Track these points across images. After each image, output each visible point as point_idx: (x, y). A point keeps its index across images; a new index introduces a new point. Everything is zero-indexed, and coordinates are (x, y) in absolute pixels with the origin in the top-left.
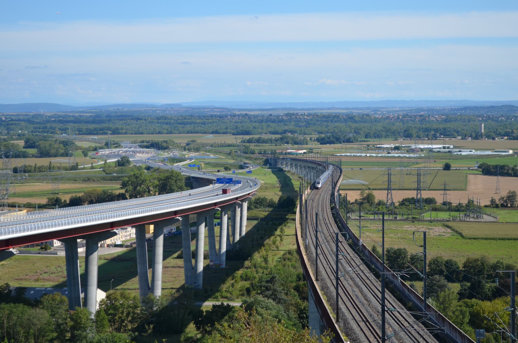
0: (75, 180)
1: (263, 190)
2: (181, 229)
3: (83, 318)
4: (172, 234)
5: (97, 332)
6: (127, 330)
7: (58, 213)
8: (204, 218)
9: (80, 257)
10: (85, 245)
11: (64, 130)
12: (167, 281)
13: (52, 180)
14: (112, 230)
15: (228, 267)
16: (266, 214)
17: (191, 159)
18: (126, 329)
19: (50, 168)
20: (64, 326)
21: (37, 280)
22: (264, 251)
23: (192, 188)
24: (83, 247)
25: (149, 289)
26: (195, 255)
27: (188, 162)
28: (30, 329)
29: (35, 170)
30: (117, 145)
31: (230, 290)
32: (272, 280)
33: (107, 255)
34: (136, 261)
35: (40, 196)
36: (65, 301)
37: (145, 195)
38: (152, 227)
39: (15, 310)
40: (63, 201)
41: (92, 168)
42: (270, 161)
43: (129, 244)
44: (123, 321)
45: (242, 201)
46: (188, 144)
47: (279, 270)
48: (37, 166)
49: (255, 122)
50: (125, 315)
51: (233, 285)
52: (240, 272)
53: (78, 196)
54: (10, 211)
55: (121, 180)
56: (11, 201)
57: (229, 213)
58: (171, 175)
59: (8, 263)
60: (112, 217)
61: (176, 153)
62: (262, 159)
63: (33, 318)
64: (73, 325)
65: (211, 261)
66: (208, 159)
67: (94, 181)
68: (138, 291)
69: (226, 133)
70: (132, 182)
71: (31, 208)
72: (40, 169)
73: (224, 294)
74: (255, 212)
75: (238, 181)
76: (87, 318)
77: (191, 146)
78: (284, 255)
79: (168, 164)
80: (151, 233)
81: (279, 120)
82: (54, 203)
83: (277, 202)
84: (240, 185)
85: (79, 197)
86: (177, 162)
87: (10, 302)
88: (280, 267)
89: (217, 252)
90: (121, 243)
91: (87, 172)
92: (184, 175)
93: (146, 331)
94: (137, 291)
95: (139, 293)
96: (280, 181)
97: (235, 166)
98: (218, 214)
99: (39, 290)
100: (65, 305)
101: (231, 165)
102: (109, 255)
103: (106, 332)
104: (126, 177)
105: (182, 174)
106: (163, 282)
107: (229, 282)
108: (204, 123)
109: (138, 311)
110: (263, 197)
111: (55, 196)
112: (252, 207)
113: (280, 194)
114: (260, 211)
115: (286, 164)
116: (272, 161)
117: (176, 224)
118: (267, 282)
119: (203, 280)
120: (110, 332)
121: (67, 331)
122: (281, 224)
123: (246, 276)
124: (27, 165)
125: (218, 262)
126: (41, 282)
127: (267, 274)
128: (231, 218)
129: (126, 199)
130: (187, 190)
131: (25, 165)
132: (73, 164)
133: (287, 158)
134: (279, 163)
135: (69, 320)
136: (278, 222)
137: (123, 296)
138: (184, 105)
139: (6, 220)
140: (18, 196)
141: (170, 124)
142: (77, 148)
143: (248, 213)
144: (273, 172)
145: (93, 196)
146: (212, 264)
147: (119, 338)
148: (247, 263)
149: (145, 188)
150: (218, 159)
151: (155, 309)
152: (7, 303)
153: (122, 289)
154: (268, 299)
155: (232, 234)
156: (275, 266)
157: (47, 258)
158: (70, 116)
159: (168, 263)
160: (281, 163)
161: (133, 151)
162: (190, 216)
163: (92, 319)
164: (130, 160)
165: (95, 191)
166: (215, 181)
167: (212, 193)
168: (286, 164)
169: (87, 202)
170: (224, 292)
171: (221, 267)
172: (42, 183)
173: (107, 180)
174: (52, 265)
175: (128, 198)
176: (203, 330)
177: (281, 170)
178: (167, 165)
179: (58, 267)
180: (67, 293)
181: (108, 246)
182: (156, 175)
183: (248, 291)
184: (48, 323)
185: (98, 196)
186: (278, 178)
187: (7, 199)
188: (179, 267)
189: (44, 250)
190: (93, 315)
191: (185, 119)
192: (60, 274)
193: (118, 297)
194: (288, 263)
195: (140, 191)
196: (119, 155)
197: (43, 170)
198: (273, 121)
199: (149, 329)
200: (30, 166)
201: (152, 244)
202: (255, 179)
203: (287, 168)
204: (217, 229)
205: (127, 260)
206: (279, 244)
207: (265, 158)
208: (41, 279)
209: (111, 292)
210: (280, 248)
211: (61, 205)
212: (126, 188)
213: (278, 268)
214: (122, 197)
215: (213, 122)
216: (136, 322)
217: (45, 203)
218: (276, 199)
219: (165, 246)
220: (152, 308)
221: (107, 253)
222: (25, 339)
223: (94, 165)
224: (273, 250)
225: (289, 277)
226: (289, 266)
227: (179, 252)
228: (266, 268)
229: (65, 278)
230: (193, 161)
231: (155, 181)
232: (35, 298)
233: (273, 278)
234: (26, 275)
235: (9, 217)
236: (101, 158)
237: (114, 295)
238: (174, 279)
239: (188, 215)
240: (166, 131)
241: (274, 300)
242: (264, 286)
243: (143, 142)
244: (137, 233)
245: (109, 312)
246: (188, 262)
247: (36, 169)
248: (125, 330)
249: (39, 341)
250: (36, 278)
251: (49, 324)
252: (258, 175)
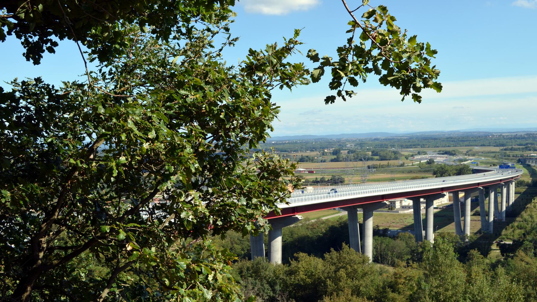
11: (393, 146)
17: (471, 160)
30: (425, 153)
41: (413, 165)
46: (467, 152)
49: (507, 139)
61: (461, 157)
69: (490, 146)
72: (382, 166)
77: (470, 153)
81: (522, 138)
96: (529, 172)
108: (475, 141)
138: (461, 131)
141: (454, 141)
142: (403, 155)
144: (524, 167)
158: (395, 139)
160: (529, 162)
161: (435, 156)
177: (529, 165)
191: (463, 138)
196: (426, 159)
198: (519, 138)
200: (377, 165)
215: (481, 140)
236: (416, 160)
240: (452, 146)
243: (440, 151)
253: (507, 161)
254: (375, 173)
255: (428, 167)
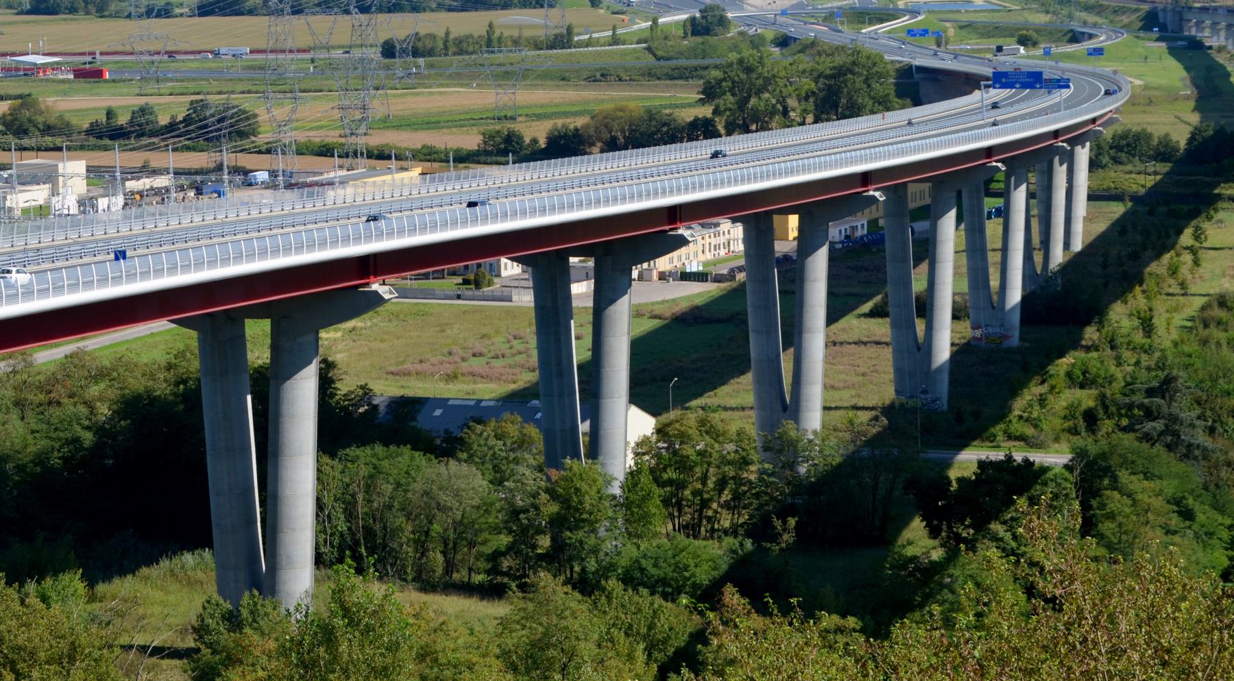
0: (563, 79)
1: (1140, 108)
2: (882, 228)
3: (587, 493)
4: (855, 242)
5: (630, 534)
6: (718, 530)
7: (513, 180)
8: (954, 194)
9: (578, 307)
10: (592, 273)
12: (841, 385)
13: (496, 77)
14: (671, 230)
15: (1027, 344)
16: (1150, 181)
18: (716, 526)
19: (489, 43)
20: (532, 513)
21: (452, 377)
22: (1140, 296)
23: (917, 102)
24: (587, 278)
25: (785, 408)
26: (925, 307)
27: (904, 21)
28: (431, 522)
29: (446, 48)
31: (1035, 415)
32: (1165, 388)
33: (658, 303)
34: (745, 322)
35: (462, 126)
36: (531, 443)
37: (774, 124)
38: (793, 220)
39: (385, 463)
40: (527, 140)
41: (615, 41)
42: (1161, 15)
43: (725, 272)
44: (705, 504)
45: (1074, 142)
47: (1190, 356)
48: (452, 36)
50: (711, 484)
51: (1042, 401)
52: (1065, 362)
53: (572, 127)
54: (373, 172)
55: (701, 77)
56: (376, 140)
57: (1033, 178)
58: (854, 63)
59: (369, 324)
60: (671, 192)
62: (1137, 10)
63: (440, 489)
64: (558, 513)
65: (975, 327)
66: (966, 11)
67: (620, 80)
68: (752, 413)
70: (733, 82)
71: (434, 161)
72: (461, 46)
73: (1018, 427)
74: (1112, 174)
75: (1058, 81)
76: (599, 492)
78: (1203, 309)
79: (845, 28)
80: (791, 238)
82: (502, 146)
83: (1183, 144)
84: (1065, 93)
85: (576, 129)
86: (871, 23)
87: (374, 443)
88: (1192, 347)
89: (995, 298)
90: (701, 268)
91: (599, 54)
92: (892, 62)
93: (775, 538)
94: (747, 412)
95: (753, 420)
97: (1050, 33)
98: (998, 181)
99: (459, 406)
100: (535, 451)
101: (1037, 31)
102: (666, 305)
103: (656, 535)
104: (716, 67)
105: (887, 58)
106: (826, 387)
107: (1035, 390)
109: (751, 474)
110: (1139, 129)
111: (505, 127)
112: (1105, 159)
113: (1195, 118)
114: (1131, 172)
115: (1214, 25)
116: (1169, 16)
117: (867, 211)
118: (1150, 392)
119: (951, 383)
120: (668, 534)
121: (540, 531)
122: (1195, 214)
123: (1084, 374)
124: (422, 32)
125: (998, 330)
126: (464, 382)
127: (1149, 369)
128: (1038, 194)
129: (720, 136)
130: (903, 107)
131: (417, 34)
132: (557, 31)
133: (1216, 9)
134: (1192, 24)
135: (544, 497)
136: (1186, 208)
137: (706, 427)
139: (359, 199)
140: (398, 127)
143: (1090, 178)
144: (1173, 52)
145: (616, 126)
146: (978, 333)
147: (696, 556)
148: (1090, 334)
149: (774, 101)
150: (999, 11)
151: (803, 469)
152: (364, 445)
153: (703, 408)
154: (1153, 444)
155: (1042, 242)
156: (1176, 344)
157: (480, 310)
159: (844, 330)
160: (1198, 24)
162: (912, 188)
163: (614, 497)
164: (729, 15)
165: (621, 110)
166: (987, 79)
167: (980, 116)
168: (1214, 25)
169: (599, 145)
170: (1015, 421)
171: (1006, 344)
172: (467, 86)
173: (659, 79)
174: (497, 332)
175: (723, 131)
176: (948, 537)
177: (1196, 45)
178: (839, 31)
179: (515, 338)
180: (539, 415)
181: (663, 276)
182: (805, 61)
183: (1091, 418)
184: (485, 504)
185: (630, 126)
186: (1187, 69)
187: (365, 134)
188: (878, 343)
189: (473, 286)
190: (616, 484)
192: (520, 359)
193: (691, 432)
194: (1217, 334)
195: (758, 111)
197: (471, 49)
199: (784, 530)
200: (432, 37)
201: (793, 270)
202: (1115, 72)
203: (1215, 38)
204: (993, 228)
205: (719, 321)
206: (1190, 277)
207: (1145, 7)
208: (463, 375)
209: (673, 414)
210: (1193, 289)
211: (522, 153)
212: (717, 101)
213: (1186, 349)
214: (702, 130)
216: (745, 507)
217: (476, 148)
218: (1181, 138)
219: (832, 278)
220: (791, 465)
221: (660, 299)
222: (416, 551)
223: (619, 31)
224: (1168, 294)
225: (1218, 378)
226: (1218, 344)
227: (879, 298)
228: (1148, 351)
229: (533, 371)
230: (920, 18)
231: (804, 80)
232: (446, 431)
233: (1168, 381)
234: (421, 362)
235: (369, 189)
237: (677, 426)
238: (861, 378)
239: (905, 183)
241: (1169, 447)
242: (1141, 406)
244: (746, 240)
245: (665, 476)
246: (903, 328)
247: (450, 44)
248: (713, 530)
249: (459, 557)
250: (450, 369)
251: (485, 507)
252: (1123, 59)
253: (1091, 18)
254: (412, 82)
255: (693, 53)
